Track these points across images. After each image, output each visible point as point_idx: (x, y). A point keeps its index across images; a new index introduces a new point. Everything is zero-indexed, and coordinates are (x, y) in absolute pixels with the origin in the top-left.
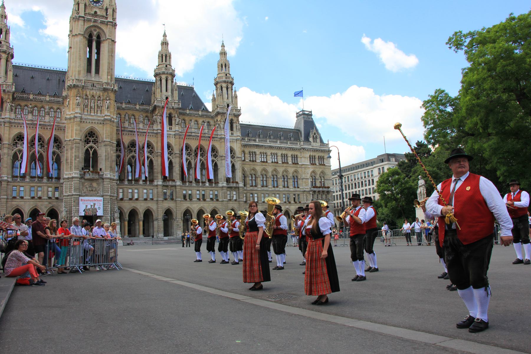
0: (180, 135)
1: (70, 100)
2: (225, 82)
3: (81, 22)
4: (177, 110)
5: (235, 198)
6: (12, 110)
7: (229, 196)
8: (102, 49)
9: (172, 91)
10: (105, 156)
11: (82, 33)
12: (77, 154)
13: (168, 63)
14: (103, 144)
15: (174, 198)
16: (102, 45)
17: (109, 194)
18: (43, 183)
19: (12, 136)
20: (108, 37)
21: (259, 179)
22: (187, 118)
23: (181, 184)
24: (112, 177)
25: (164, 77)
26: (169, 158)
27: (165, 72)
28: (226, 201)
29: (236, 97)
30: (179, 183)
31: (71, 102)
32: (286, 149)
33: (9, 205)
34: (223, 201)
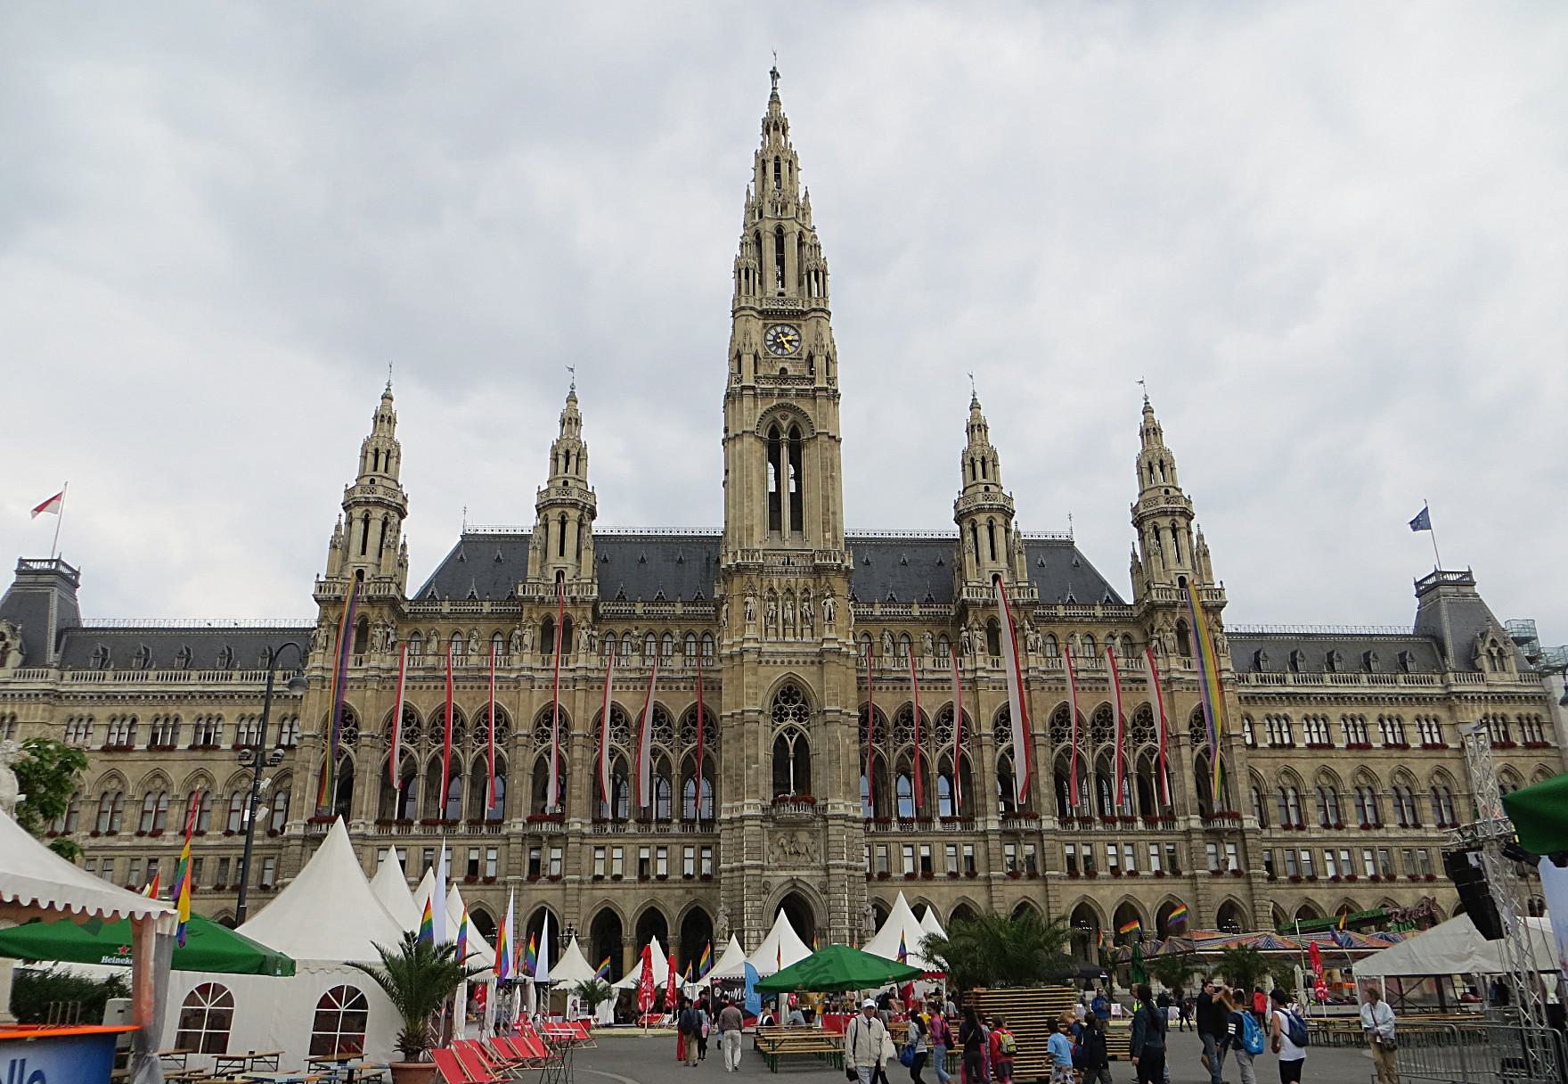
0: (1044, 681)
1: (731, 605)
2: (1164, 513)
3: (747, 402)
4: (1028, 608)
5: (1232, 865)
6: (592, 646)
7: (1212, 859)
8: (805, 463)
11: (753, 428)
12: (751, 752)
13: (990, 479)
14: (820, 720)
15: (1039, 869)
16: (804, 452)
17: (844, 862)
18: (672, 836)
21: (1309, 802)
22: (1060, 631)
23: (1058, 827)
24: (851, 813)
25: (982, 519)
27: (983, 506)
28: (1204, 876)
29: (1206, 554)
30: (1049, 823)
32: (1392, 700)
33: (584, 899)
34: (1193, 877)
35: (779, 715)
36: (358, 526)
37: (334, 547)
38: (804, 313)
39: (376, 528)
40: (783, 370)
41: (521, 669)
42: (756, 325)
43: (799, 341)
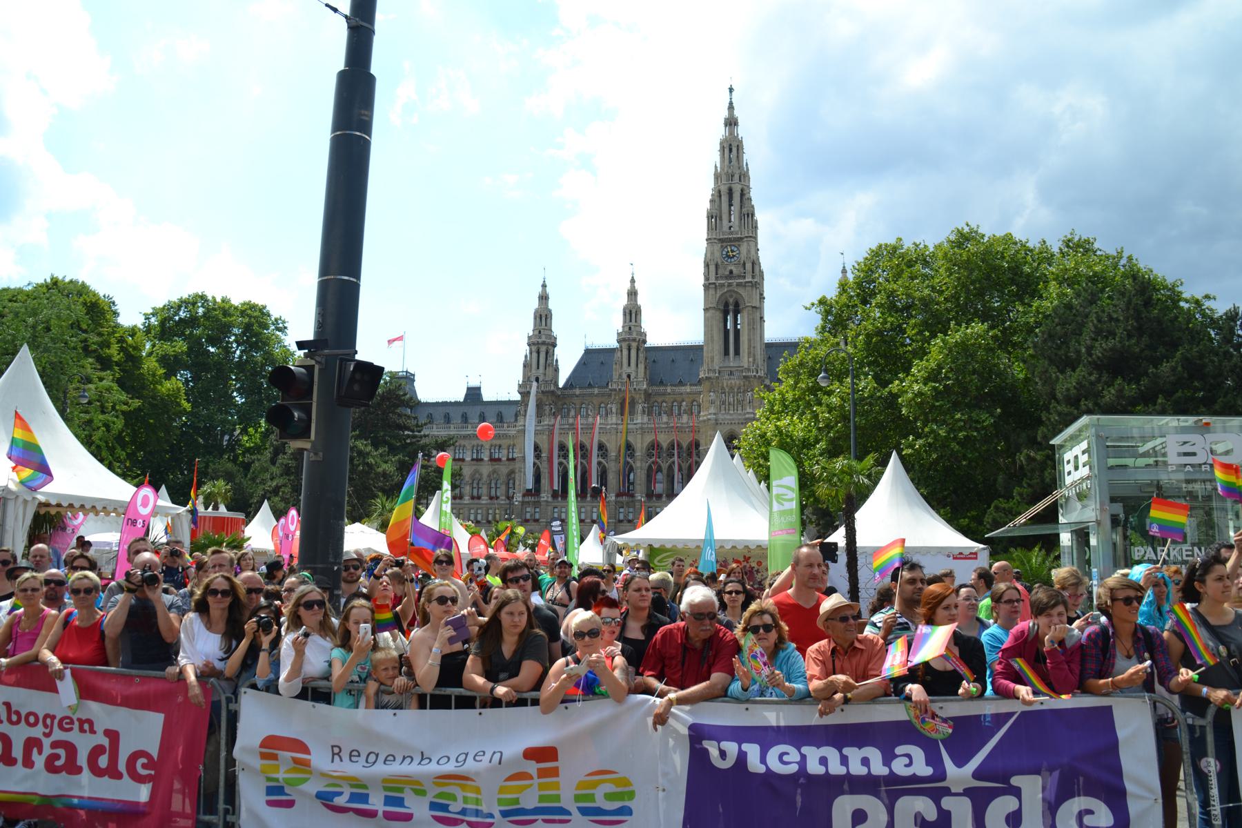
19: (645, 445)
36: (535, 355)
37: (525, 366)
38: (740, 239)
39: (542, 355)
42: (717, 247)
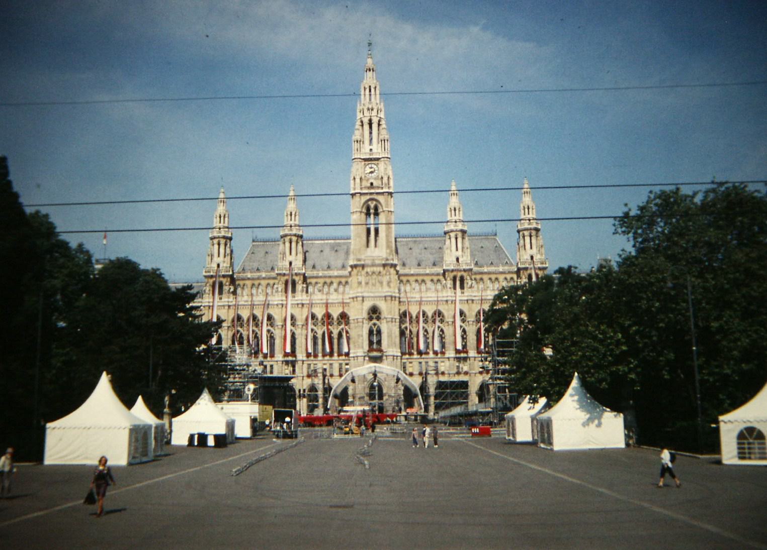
6: (302, 291)
9: (463, 248)
10: (388, 333)
12: (360, 333)
14: (385, 321)
20: (384, 209)
26: (461, 327)
31: (353, 281)
35: (371, 319)
36: (216, 246)
40: (372, 184)
41: (278, 300)
43: (378, 170)
